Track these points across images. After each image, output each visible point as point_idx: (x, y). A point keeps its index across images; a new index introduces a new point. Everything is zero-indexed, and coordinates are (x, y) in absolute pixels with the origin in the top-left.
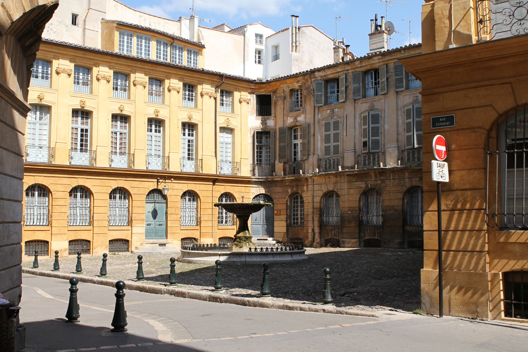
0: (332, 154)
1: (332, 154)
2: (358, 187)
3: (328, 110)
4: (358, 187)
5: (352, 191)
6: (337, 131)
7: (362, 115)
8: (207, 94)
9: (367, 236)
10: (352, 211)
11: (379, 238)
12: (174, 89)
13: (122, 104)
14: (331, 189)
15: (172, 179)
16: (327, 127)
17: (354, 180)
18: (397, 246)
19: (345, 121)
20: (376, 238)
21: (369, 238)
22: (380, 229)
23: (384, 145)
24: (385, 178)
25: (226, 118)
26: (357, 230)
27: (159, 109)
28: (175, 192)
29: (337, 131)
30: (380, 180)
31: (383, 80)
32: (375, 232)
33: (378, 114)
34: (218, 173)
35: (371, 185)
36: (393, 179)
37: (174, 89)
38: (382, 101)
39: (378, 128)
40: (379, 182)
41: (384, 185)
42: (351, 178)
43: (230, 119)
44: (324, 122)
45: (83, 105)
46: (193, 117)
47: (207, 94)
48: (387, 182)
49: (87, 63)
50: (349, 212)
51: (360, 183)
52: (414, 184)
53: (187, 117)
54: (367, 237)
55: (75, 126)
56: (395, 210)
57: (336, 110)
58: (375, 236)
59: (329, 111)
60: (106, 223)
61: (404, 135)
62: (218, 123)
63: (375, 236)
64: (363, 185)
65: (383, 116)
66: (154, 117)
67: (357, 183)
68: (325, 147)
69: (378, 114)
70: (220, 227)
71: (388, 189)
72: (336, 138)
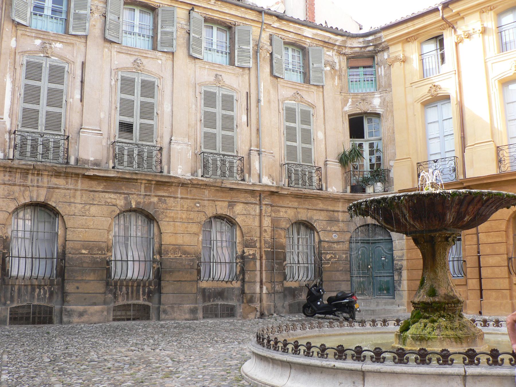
0: (41, 128)
1: (41, 128)
2: (107, 204)
3: (40, 38)
4: (107, 204)
5: (93, 210)
6: (59, 87)
7: (120, 73)
9: (120, 299)
10: (90, 249)
11: (147, 303)
14: (42, 199)
16: (33, 70)
17: (100, 189)
18: (187, 316)
19: (79, 72)
20: (141, 302)
21: (125, 302)
22: (150, 284)
23: (162, 137)
24: (165, 194)
26: (100, 287)
29: (59, 87)
30: (156, 196)
31: (168, 29)
32: (138, 291)
33: (154, 83)
35: (138, 203)
36: (182, 198)
38: (160, 62)
39: (151, 106)
40: (155, 200)
41: (164, 206)
42: (94, 183)
44: (24, 60)
48: (170, 202)
50: (84, 251)
51: (112, 196)
52: (220, 212)
54: (121, 302)
56: (185, 253)
57: (59, 45)
58: (138, 299)
59: (38, 42)
61: (201, 130)
63: (138, 299)
64: (121, 202)
65: (160, 87)
67: (107, 195)
68: (25, 110)
69: (154, 83)
71: (172, 215)
72: (56, 98)
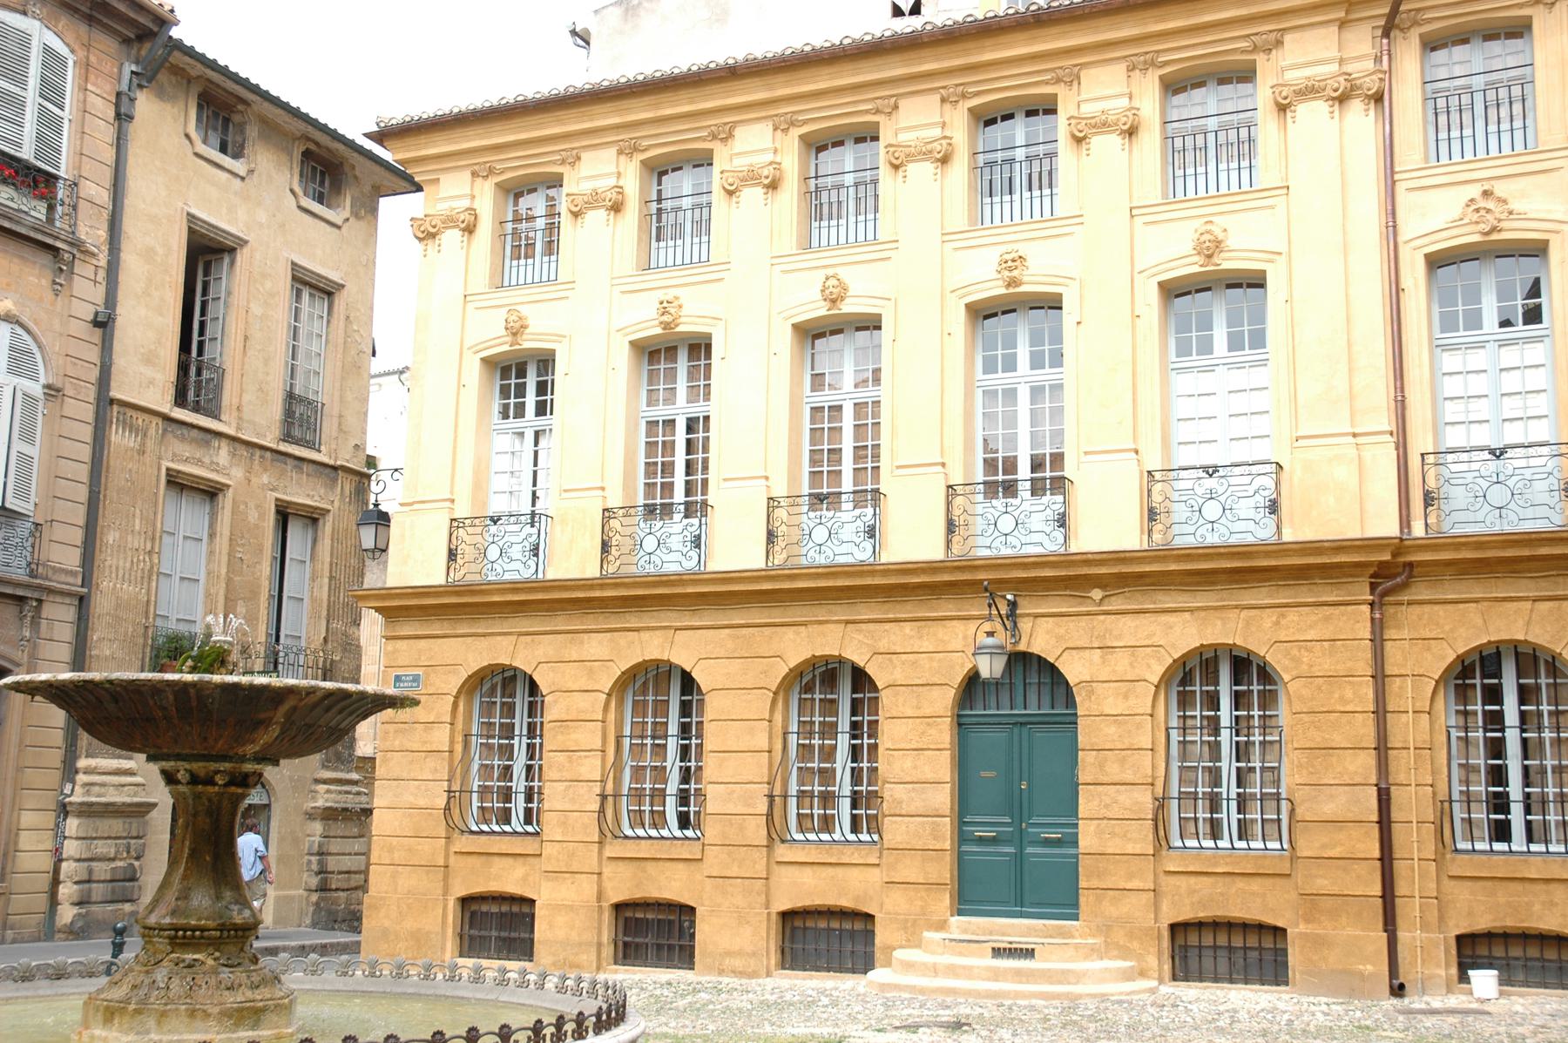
8: (1309, 91)
12: (1103, 126)
13: (830, 272)
15: (1097, 594)
25: (1475, 191)
27: (1023, 249)
28: (1121, 664)
34: (1418, 530)
37: (1103, 126)
43: (1500, 189)
45: (666, 318)
46: (1231, 242)
47: (1309, 91)
49: (688, 138)
53: (1188, 248)
55: (661, 412)
60: (756, 831)
62: (1407, 230)
66: (1003, 291)
70: (1460, 866)
